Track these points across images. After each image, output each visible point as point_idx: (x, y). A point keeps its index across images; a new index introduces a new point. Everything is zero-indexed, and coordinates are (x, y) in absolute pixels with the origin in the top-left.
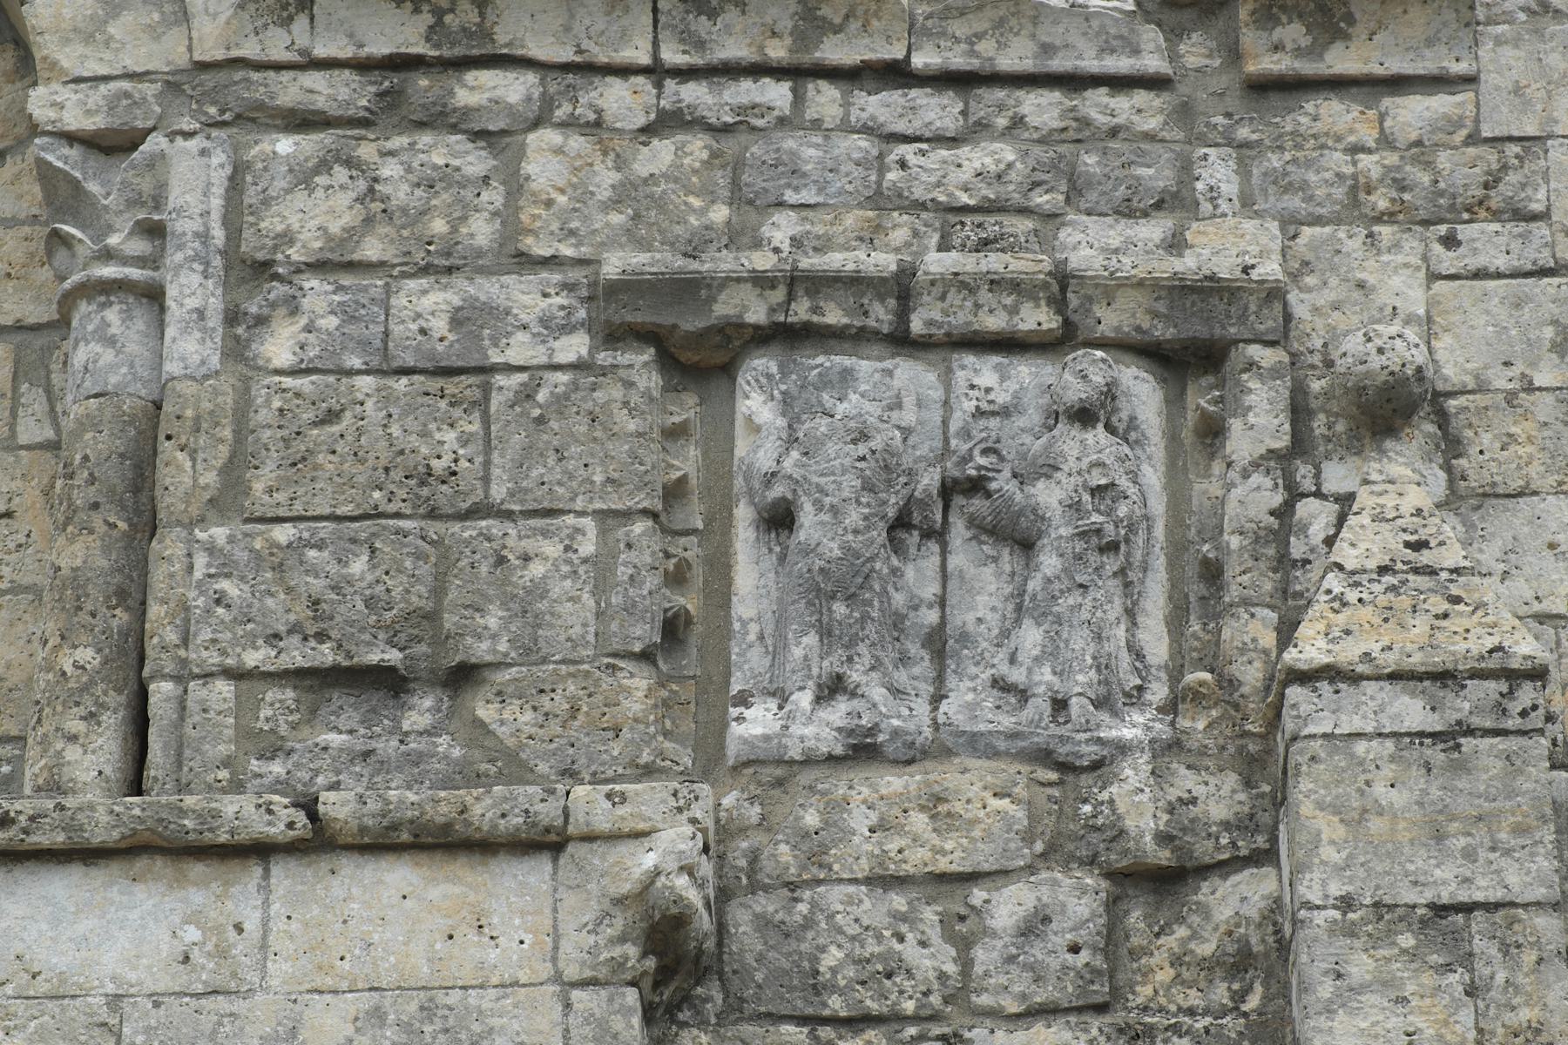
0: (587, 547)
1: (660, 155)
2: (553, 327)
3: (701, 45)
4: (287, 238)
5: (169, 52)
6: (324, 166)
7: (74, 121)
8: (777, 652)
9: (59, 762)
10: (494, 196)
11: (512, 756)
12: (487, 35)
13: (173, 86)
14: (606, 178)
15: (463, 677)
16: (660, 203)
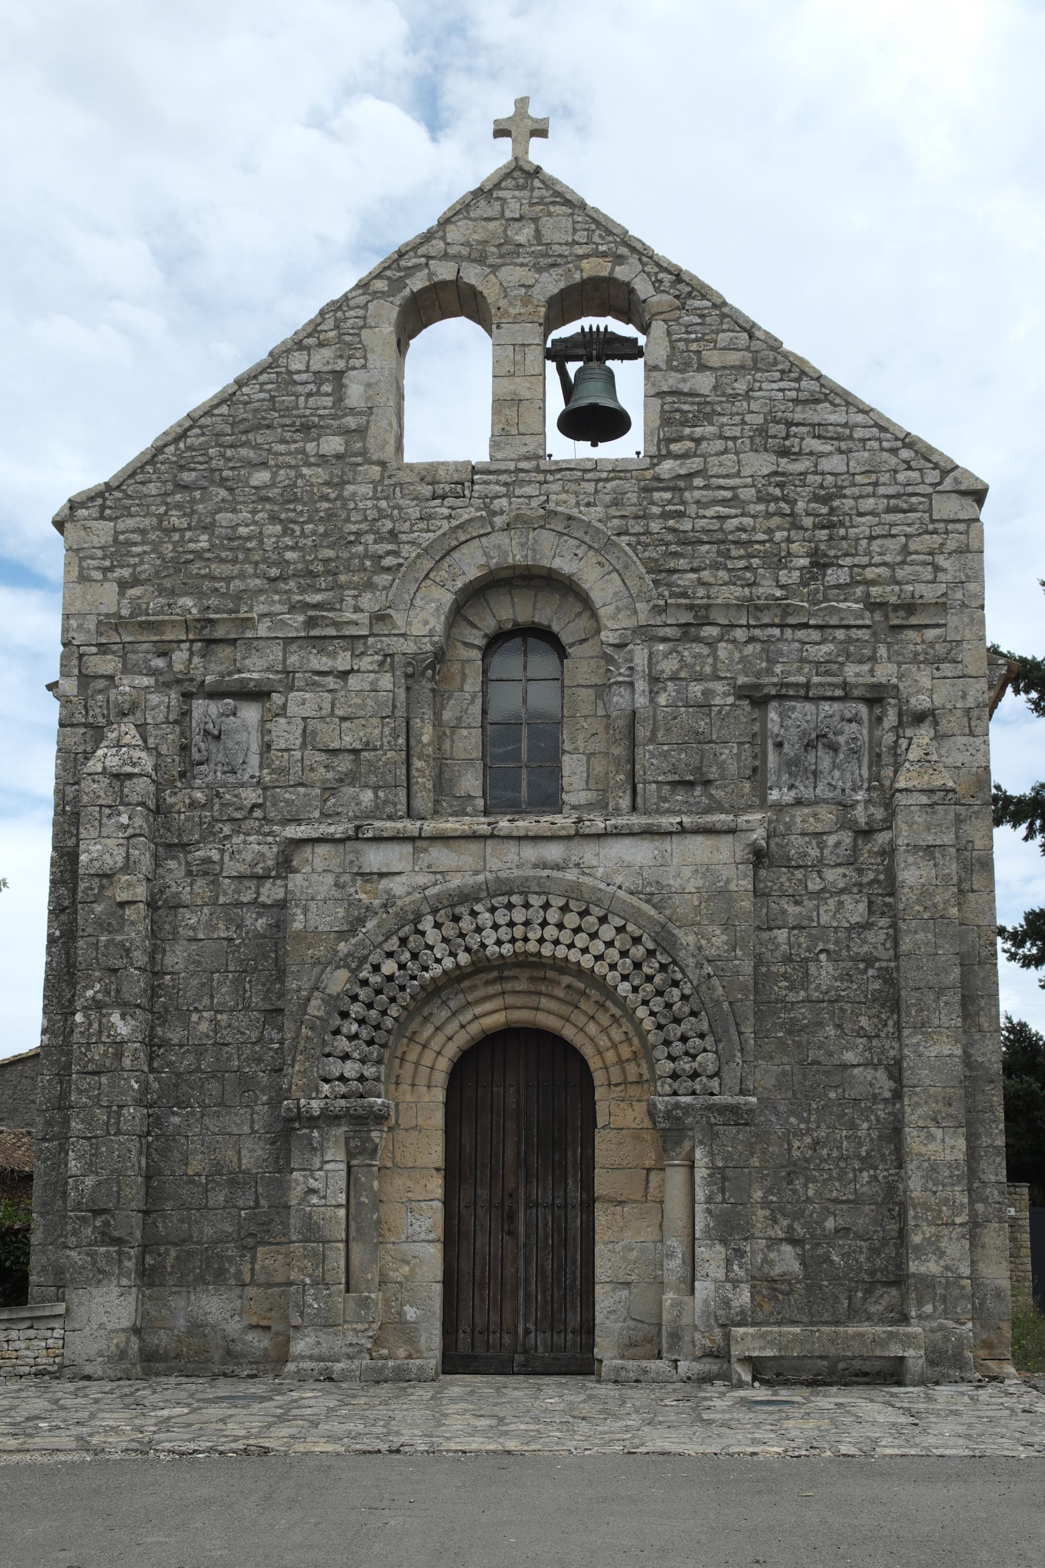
0: (735, 751)
1: (749, 649)
2: (726, 695)
3: (759, 619)
4: (663, 671)
5: (631, 623)
6: (671, 653)
7: (612, 641)
8: (779, 777)
9: (617, 804)
10: (710, 660)
11: (719, 803)
12: (707, 617)
13: (634, 632)
14: (737, 655)
15: (707, 783)
16: (750, 662)
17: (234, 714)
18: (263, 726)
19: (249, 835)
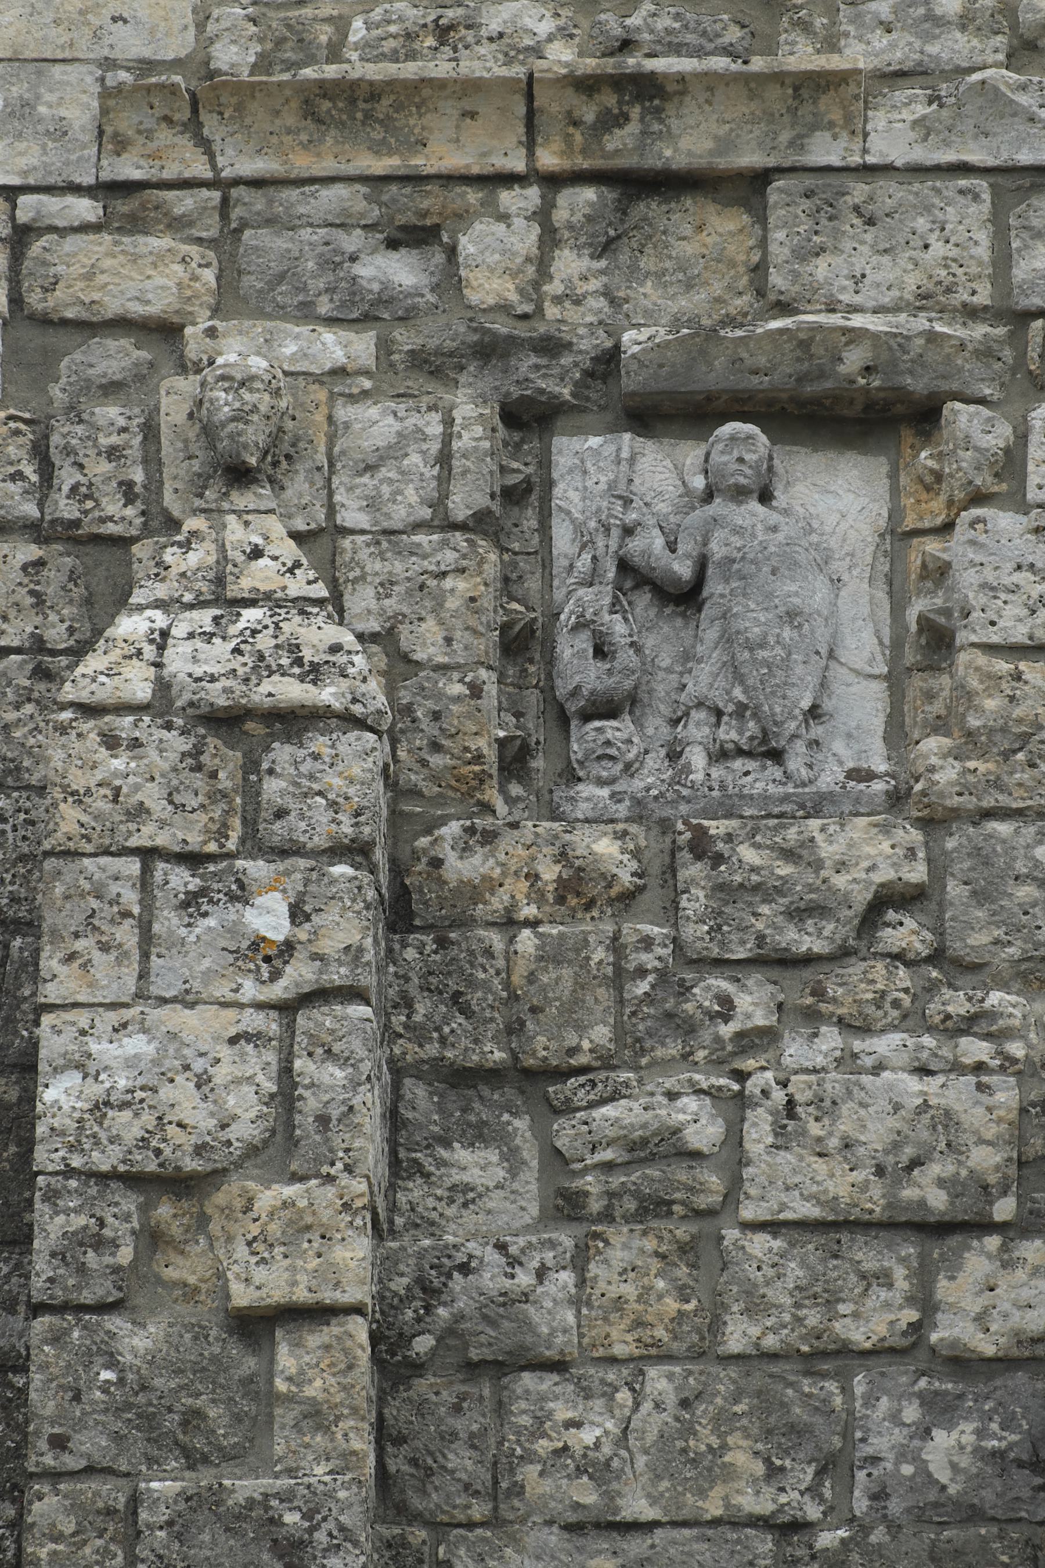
17: (765, 497)
18: (896, 558)
19: (865, 1030)
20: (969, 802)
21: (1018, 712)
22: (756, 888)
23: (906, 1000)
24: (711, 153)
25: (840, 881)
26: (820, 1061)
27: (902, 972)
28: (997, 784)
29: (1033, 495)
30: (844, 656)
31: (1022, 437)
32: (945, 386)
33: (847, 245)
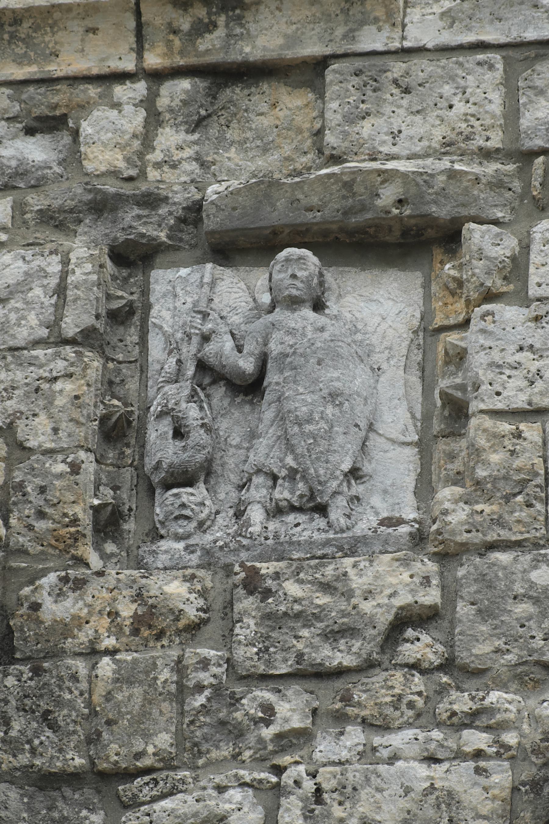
20: (476, 538)
21: (517, 463)
22: (298, 616)
23: (420, 702)
24: (281, 47)
25: (367, 607)
26: (345, 755)
27: (417, 678)
28: (499, 522)
29: (533, 291)
30: (381, 428)
31: (526, 248)
32: (464, 212)
33: (387, 109)
